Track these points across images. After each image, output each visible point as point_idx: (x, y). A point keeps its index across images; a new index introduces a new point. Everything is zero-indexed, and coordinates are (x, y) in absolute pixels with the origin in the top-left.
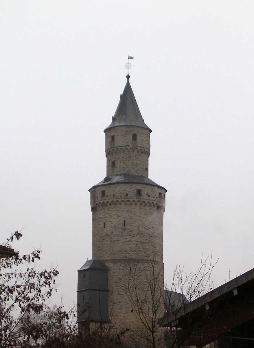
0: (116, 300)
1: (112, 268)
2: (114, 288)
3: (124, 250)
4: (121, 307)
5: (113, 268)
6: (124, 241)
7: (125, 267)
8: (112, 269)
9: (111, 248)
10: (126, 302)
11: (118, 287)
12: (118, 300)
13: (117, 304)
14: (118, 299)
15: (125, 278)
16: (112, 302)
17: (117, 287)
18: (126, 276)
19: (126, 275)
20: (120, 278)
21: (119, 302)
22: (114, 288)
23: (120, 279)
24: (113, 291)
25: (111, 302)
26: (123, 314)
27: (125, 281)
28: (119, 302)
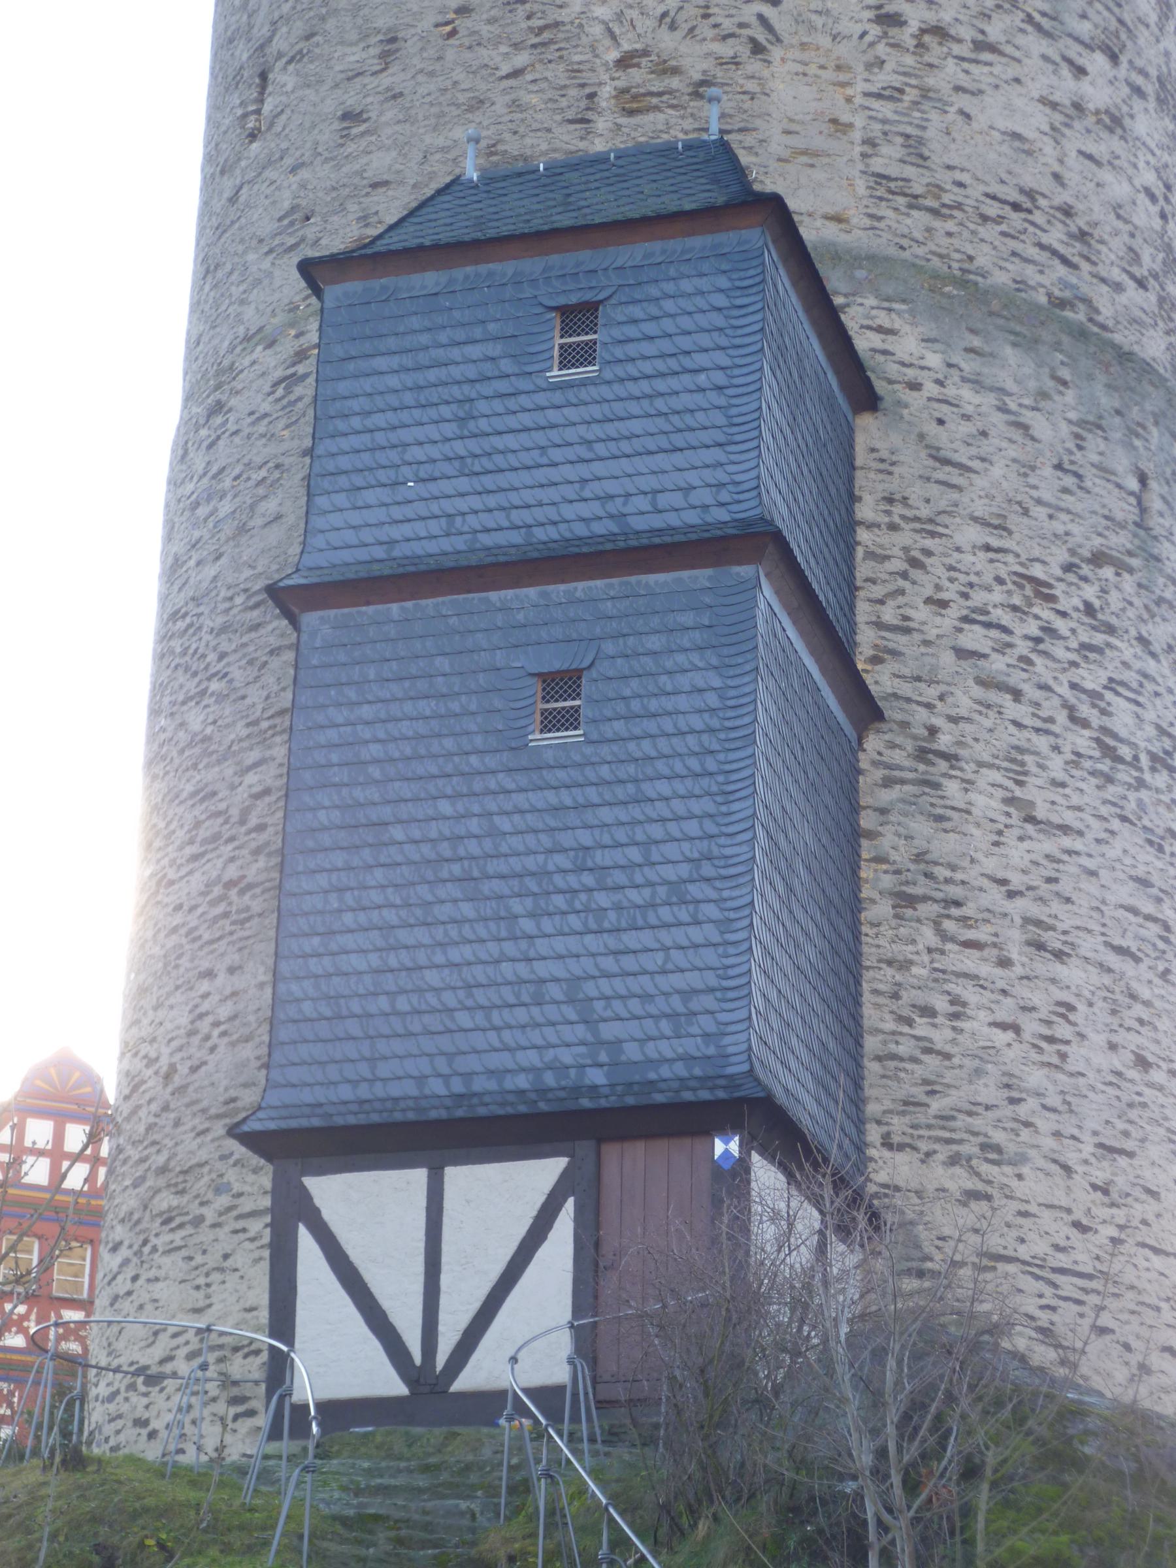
0: (994, 896)
1: (915, 386)
2: (963, 703)
3: (1067, 211)
4: (1062, 1030)
5: (930, 389)
6: (1066, 87)
7: (1094, 442)
8: (915, 400)
9: (885, 109)
10: (1112, 960)
11: (1017, 695)
12: (1011, 895)
13: (1004, 963)
14: (1017, 881)
15: (1090, 592)
16: (927, 910)
17: (993, 696)
18: (1108, 572)
19: (1098, 559)
20: (1037, 571)
21: (1040, 946)
22: (963, 703)
23: (1042, 591)
24: (933, 731)
25: (905, 900)
26: (1088, 1149)
27: (1099, 639)
28: (1040, 946)
